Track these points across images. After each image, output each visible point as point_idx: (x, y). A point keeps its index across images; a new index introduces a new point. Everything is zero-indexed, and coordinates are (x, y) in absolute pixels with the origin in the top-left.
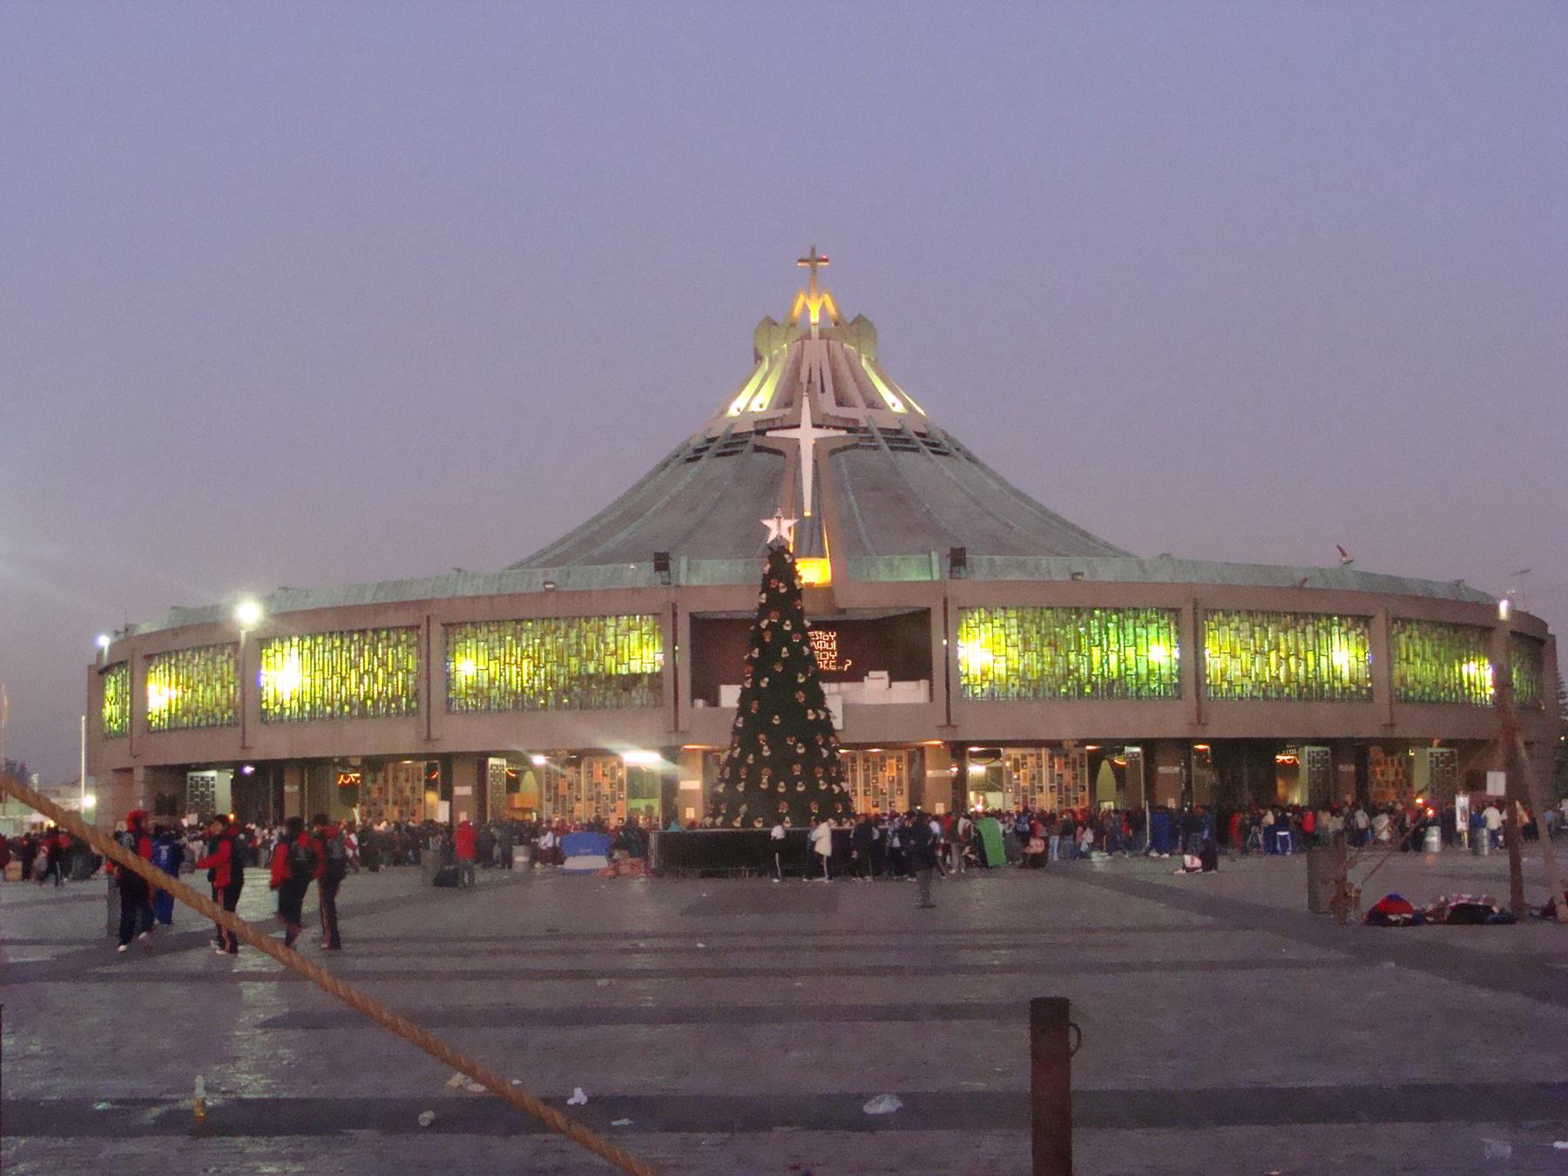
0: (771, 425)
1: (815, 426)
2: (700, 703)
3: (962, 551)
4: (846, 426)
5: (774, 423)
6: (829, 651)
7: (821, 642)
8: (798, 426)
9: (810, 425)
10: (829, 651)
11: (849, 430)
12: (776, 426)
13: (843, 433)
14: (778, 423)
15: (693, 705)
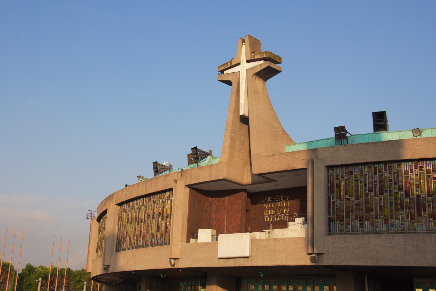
0: (226, 67)
1: (248, 61)
2: (192, 241)
3: (343, 128)
4: (262, 57)
5: (227, 66)
6: (285, 208)
7: (281, 202)
8: (239, 64)
9: (245, 61)
10: (285, 208)
11: (265, 59)
12: (228, 66)
13: (262, 62)
14: (229, 66)
15: (188, 241)
